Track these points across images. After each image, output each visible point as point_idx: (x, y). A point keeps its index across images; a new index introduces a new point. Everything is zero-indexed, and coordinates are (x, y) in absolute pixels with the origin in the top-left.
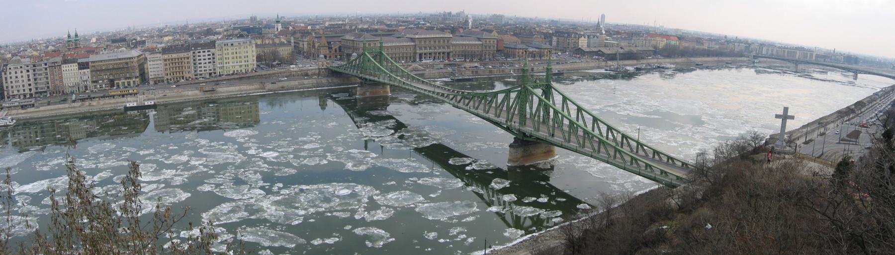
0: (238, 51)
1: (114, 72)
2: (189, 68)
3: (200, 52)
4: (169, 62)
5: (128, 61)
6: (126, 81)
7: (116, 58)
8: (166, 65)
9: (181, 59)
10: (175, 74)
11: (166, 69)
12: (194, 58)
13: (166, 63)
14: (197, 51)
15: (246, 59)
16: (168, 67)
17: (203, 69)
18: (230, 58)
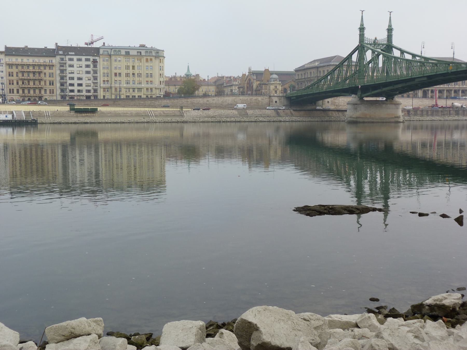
0: (137, 64)
2: (52, 83)
4: (17, 70)
8: (10, 74)
9: (39, 68)
10: (26, 91)
14: (68, 57)
15: (149, 79)
17: (76, 88)
18: (123, 75)
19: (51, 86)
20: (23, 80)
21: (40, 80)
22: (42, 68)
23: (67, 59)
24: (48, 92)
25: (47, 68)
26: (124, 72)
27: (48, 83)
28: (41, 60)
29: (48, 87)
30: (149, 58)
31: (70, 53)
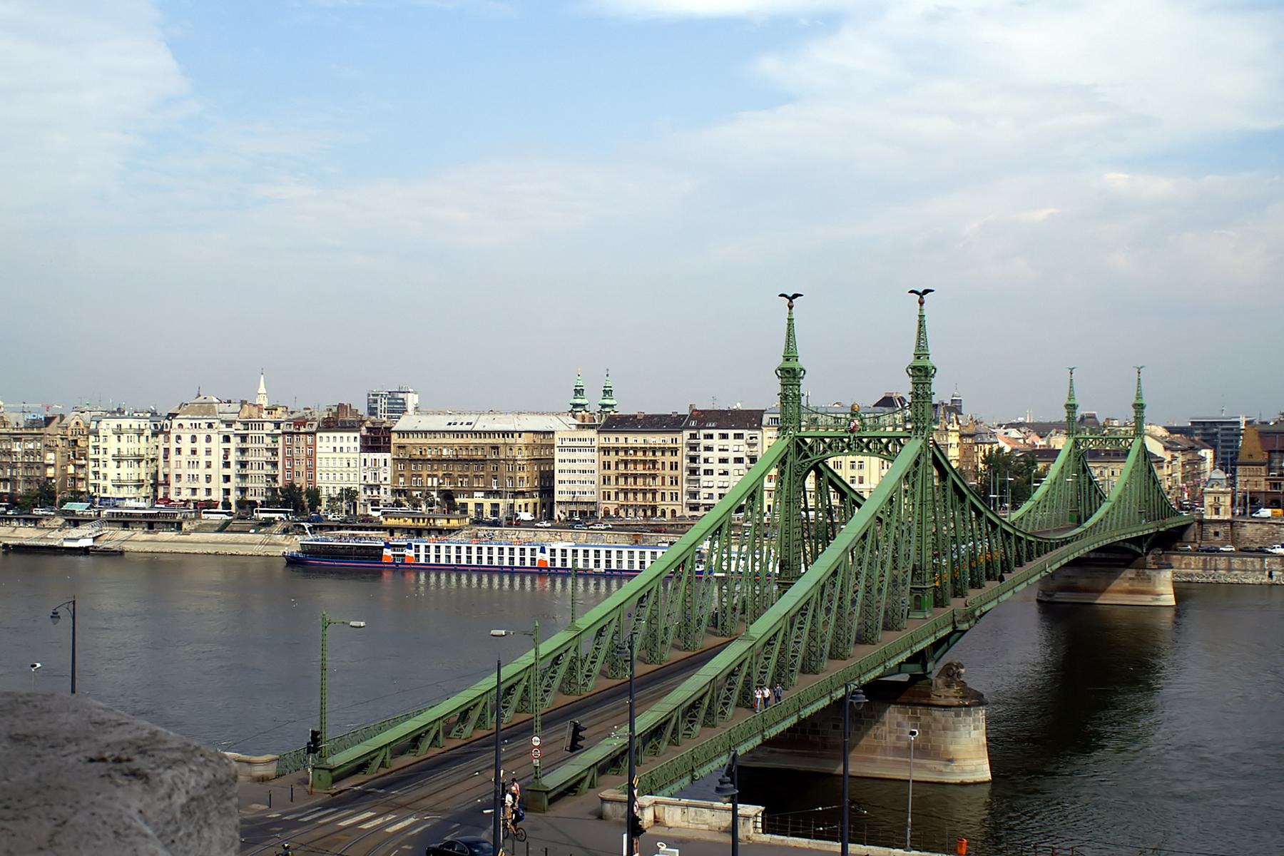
1: (456, 470)
3: (711, 437)
4: (616, 458)
5: (499, 440)
6: (487, 504)
7: (469, 428)
8: (607, 466)
9: (654, 454)
11: (606, 480)
12: (692, 453)
13: (607, 458)
16: (612, 472)
20: (626, 477)
21: (654, 477)
22: (659, 454)
23: (702, 437)
24: (668, 497)
25: (668, 454)
27: (668, 480)
28: (656, 440)
29: (668, 488)
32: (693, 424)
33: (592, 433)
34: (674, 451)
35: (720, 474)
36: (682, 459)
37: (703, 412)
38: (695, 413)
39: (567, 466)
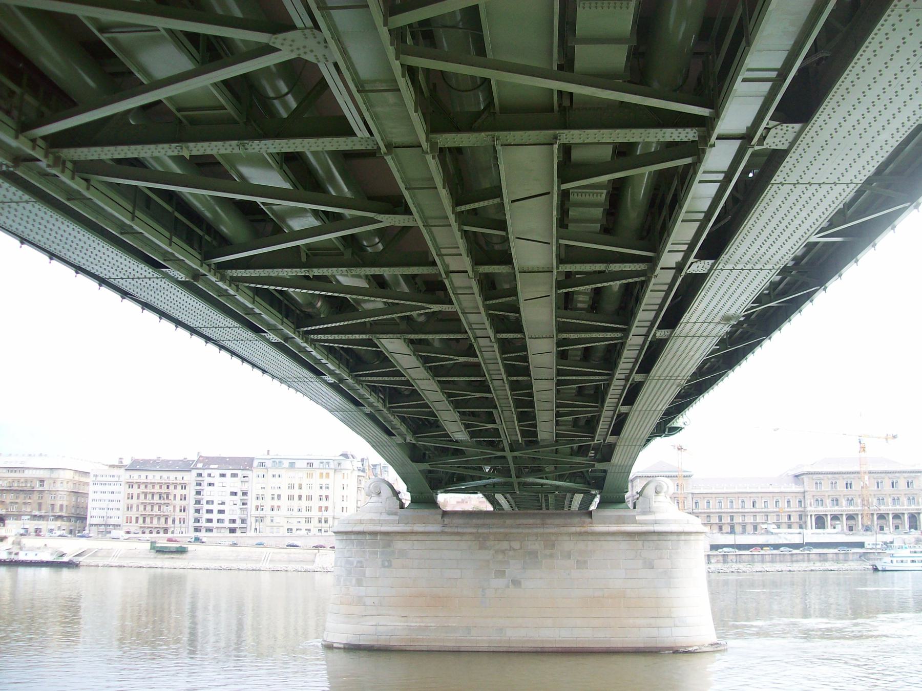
10: (148, 520)
11: (129, 508)
13: (131, 491)
15: (324, 504)
16: (135, 501)
19: (182, 513)
20: (145, 505)
26: (285, 493)
27: (178, 509)
28: (172, 477)
30: (324, 472)
31: (212, 466)
32: (200, 465)
33: (122, 472)
34: (184, 487)
35: (219, 504)
36: (191, 492)
37: (207, 458)
38: (201, 458)
39: (98, 496)
